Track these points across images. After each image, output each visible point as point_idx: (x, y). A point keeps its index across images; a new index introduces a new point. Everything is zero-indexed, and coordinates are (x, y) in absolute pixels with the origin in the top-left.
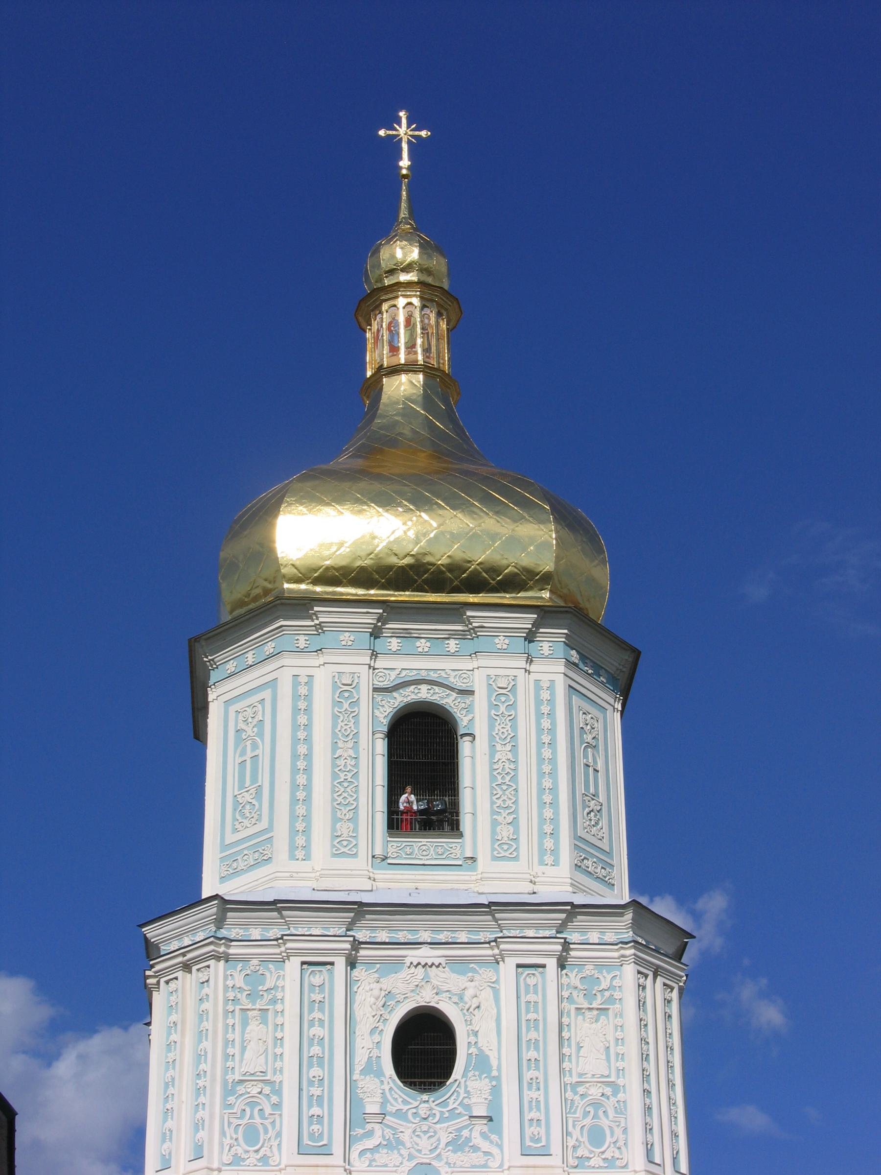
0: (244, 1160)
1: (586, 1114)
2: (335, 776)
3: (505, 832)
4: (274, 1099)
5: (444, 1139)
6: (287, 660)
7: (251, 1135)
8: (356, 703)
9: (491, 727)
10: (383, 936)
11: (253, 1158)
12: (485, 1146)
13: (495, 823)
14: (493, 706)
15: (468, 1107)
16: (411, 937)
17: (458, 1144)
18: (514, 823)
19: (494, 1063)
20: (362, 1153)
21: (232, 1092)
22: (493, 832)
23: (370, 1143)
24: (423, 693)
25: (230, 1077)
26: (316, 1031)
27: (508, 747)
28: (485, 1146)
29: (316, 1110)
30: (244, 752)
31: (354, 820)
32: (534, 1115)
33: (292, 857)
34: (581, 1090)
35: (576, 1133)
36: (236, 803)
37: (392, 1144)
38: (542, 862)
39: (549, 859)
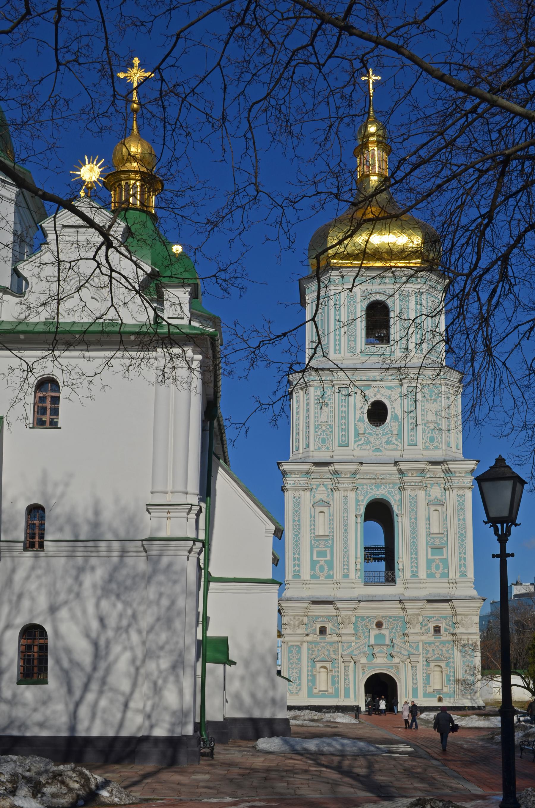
1: (429, 432)
4: (331, 430)
5: (384, 441)
7: (324, 441)
10: (364, 378)
11: (324, 448)
12: (396, 443)
15: (391, 431)
16: (373, 378)
17: (388, 442)
19: (400, 417)
20: (358, 446)
21: (318, 428)
23: (360, 443)
25: (316, 423)
26: (344, 409)
28: (396, 443)
29: (343, 433)
31: (355, 341)
32: (412, 433)
33: (335, 353)
34: (427, 425)
35: (425, 439)
37: (368, 443)
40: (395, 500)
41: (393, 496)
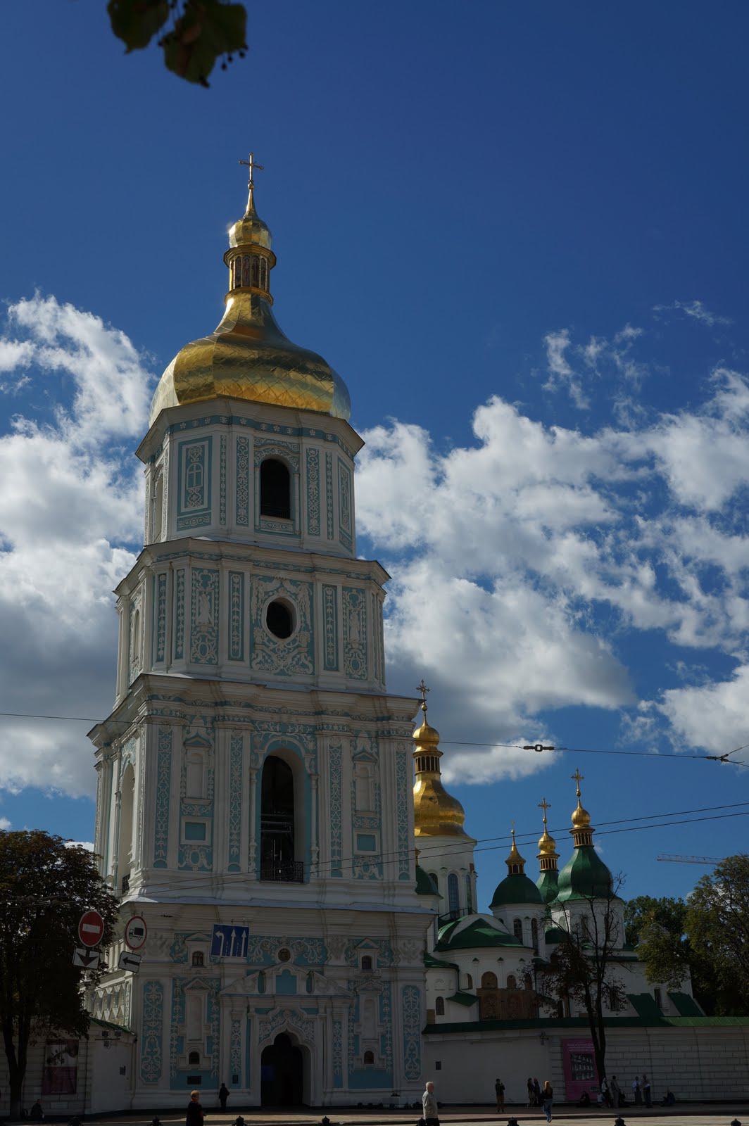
0: (200, 660)
2: (238, 487)
3: (314, 523)
6: (217, 427)
8: (247, 453)
9: (308, 472)
13: (309, 518)
14: (308, 463)
18: (318, 519)
22: (309, 522)
24: (276, 452)
27: (316, 483)
30: (192, 469)
36: (186, 491)
38: (328, 538)
39: (331, 537)
40: (307, 751)
41: (304, 746)
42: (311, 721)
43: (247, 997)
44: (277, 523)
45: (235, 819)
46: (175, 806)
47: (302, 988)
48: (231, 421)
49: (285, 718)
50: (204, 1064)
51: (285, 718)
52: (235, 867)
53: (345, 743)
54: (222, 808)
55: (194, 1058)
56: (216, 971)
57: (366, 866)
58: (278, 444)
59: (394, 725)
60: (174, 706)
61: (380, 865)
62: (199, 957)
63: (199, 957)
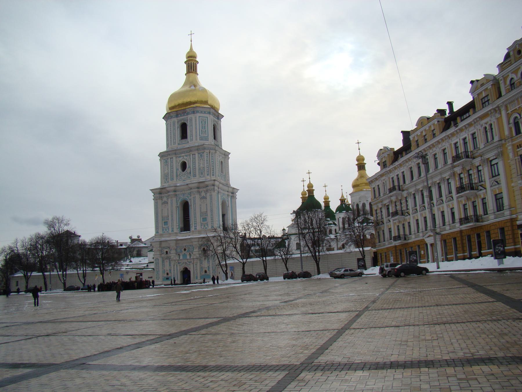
42: (189, 191)
43: (175, 260)
44: (184, 140)
45: (172, 220)
46: (160, 218)
47: (188, 257)
48: (171, 117)
49: (183, 192)
50: (170, 275)
51: (183, 192)
52: (173, 231)
53: (197, 196)
54: (170, 217)
55: (168, 274)
56: (170, 255)
57: (204, 226)
58: (183, 119)
59: (209, 188)
60: (158, 195)
61: (208, 225)
62: (167, 252)
63: (167, 252)
